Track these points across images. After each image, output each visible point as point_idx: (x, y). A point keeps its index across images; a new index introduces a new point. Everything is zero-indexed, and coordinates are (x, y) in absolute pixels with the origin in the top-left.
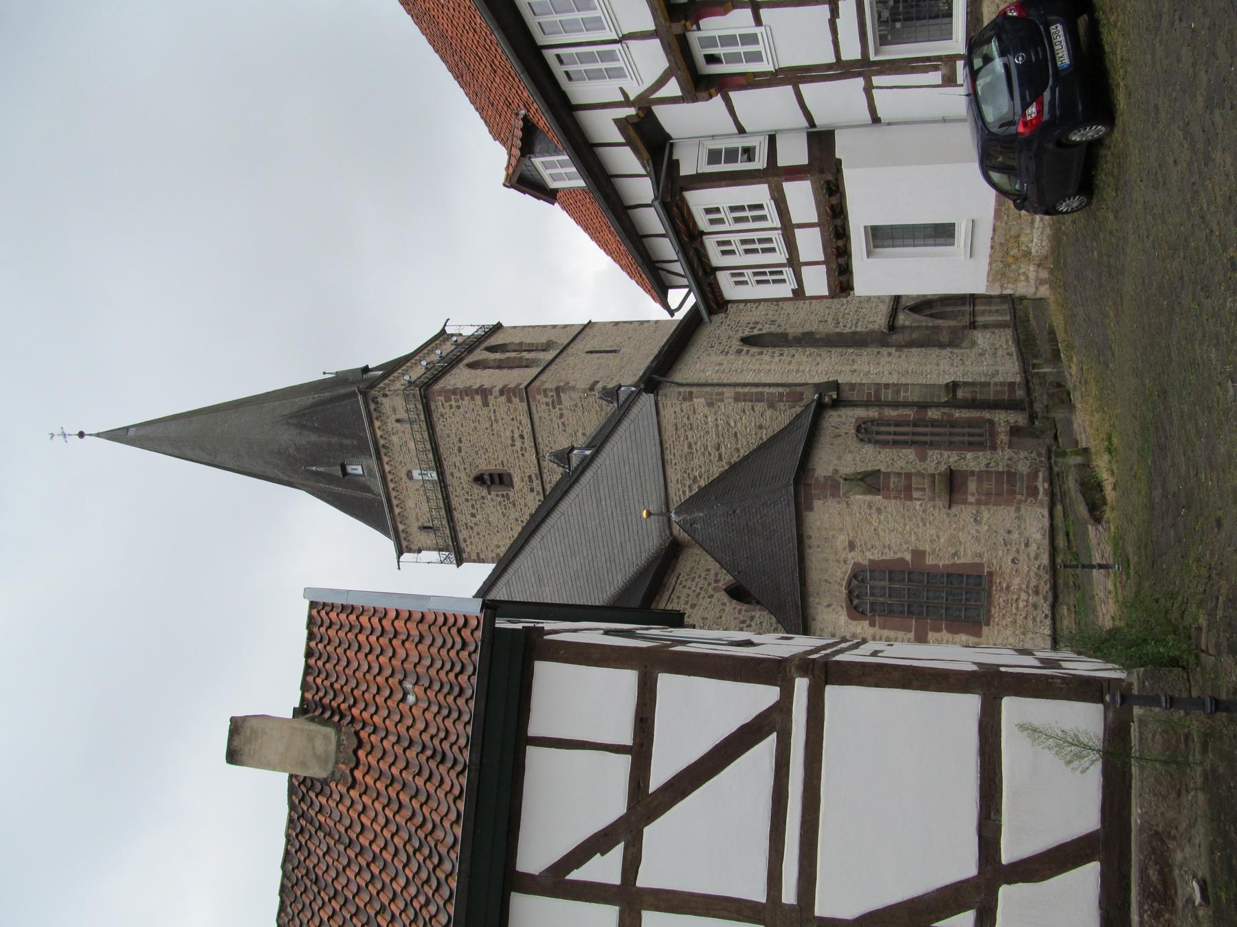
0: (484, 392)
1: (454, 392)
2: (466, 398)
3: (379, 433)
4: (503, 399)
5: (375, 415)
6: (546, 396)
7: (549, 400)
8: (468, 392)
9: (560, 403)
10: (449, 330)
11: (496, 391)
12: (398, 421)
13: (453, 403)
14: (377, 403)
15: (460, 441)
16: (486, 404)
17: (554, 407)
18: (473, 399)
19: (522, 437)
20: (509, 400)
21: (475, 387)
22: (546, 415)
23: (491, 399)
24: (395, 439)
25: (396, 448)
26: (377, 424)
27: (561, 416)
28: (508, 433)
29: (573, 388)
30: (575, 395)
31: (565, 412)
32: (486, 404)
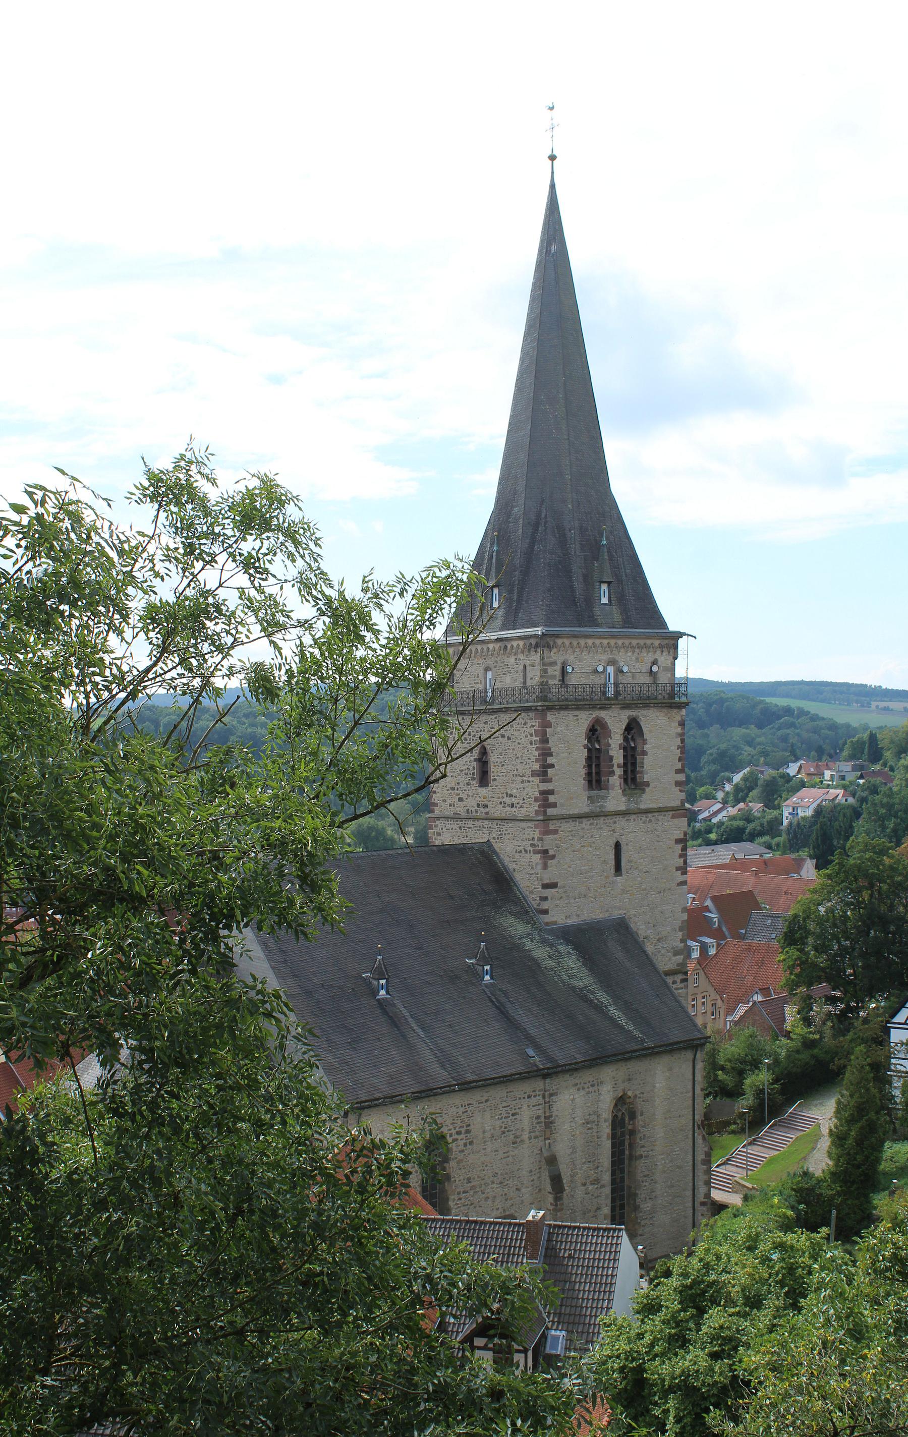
0: (543, 773)
1: (545, 740)
2: (536, 753)
3: (515, 644)
4: (537, 794)
5: (528, 642)
6: (540, 839)
7: (535, 842)
8: (546, 753)
9: (535, 852)
10: (682, 642)
11: (544, 787)
12: (525, 667)
13: (534, 738)
14: (537, 646)
15: (509, 738)
16: (534, 773)
17: (532, 845)
18: (537, 761)
19: (512, 806)
20: (536, 800)
21: (550, 760)
22: (526, 836)
23: (536, 780)
24: (512, 660)
25: (506, 660)
26: (521, 643)
27: (526, 851)
28: (514, 792)
29: (545, 867)
30: (540, 867)
31: (528, 855)
32: (534, 773)
